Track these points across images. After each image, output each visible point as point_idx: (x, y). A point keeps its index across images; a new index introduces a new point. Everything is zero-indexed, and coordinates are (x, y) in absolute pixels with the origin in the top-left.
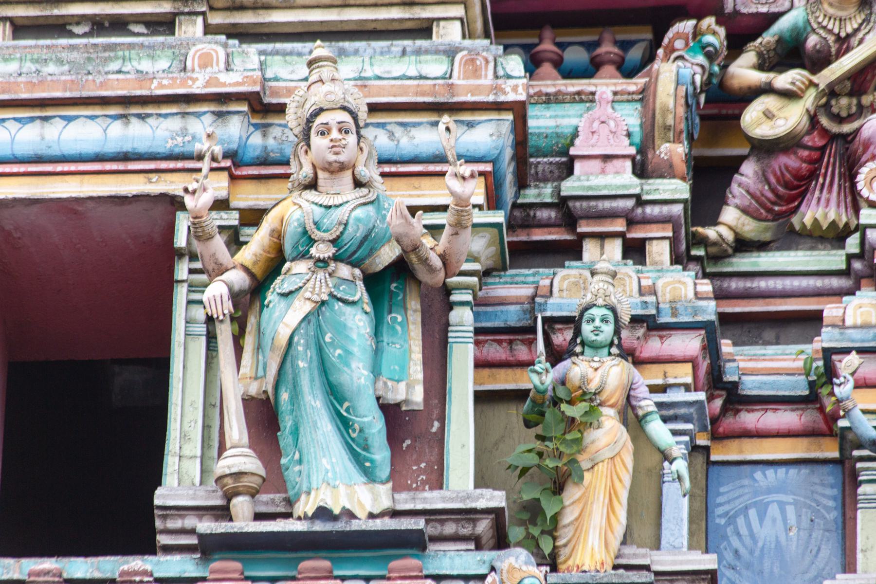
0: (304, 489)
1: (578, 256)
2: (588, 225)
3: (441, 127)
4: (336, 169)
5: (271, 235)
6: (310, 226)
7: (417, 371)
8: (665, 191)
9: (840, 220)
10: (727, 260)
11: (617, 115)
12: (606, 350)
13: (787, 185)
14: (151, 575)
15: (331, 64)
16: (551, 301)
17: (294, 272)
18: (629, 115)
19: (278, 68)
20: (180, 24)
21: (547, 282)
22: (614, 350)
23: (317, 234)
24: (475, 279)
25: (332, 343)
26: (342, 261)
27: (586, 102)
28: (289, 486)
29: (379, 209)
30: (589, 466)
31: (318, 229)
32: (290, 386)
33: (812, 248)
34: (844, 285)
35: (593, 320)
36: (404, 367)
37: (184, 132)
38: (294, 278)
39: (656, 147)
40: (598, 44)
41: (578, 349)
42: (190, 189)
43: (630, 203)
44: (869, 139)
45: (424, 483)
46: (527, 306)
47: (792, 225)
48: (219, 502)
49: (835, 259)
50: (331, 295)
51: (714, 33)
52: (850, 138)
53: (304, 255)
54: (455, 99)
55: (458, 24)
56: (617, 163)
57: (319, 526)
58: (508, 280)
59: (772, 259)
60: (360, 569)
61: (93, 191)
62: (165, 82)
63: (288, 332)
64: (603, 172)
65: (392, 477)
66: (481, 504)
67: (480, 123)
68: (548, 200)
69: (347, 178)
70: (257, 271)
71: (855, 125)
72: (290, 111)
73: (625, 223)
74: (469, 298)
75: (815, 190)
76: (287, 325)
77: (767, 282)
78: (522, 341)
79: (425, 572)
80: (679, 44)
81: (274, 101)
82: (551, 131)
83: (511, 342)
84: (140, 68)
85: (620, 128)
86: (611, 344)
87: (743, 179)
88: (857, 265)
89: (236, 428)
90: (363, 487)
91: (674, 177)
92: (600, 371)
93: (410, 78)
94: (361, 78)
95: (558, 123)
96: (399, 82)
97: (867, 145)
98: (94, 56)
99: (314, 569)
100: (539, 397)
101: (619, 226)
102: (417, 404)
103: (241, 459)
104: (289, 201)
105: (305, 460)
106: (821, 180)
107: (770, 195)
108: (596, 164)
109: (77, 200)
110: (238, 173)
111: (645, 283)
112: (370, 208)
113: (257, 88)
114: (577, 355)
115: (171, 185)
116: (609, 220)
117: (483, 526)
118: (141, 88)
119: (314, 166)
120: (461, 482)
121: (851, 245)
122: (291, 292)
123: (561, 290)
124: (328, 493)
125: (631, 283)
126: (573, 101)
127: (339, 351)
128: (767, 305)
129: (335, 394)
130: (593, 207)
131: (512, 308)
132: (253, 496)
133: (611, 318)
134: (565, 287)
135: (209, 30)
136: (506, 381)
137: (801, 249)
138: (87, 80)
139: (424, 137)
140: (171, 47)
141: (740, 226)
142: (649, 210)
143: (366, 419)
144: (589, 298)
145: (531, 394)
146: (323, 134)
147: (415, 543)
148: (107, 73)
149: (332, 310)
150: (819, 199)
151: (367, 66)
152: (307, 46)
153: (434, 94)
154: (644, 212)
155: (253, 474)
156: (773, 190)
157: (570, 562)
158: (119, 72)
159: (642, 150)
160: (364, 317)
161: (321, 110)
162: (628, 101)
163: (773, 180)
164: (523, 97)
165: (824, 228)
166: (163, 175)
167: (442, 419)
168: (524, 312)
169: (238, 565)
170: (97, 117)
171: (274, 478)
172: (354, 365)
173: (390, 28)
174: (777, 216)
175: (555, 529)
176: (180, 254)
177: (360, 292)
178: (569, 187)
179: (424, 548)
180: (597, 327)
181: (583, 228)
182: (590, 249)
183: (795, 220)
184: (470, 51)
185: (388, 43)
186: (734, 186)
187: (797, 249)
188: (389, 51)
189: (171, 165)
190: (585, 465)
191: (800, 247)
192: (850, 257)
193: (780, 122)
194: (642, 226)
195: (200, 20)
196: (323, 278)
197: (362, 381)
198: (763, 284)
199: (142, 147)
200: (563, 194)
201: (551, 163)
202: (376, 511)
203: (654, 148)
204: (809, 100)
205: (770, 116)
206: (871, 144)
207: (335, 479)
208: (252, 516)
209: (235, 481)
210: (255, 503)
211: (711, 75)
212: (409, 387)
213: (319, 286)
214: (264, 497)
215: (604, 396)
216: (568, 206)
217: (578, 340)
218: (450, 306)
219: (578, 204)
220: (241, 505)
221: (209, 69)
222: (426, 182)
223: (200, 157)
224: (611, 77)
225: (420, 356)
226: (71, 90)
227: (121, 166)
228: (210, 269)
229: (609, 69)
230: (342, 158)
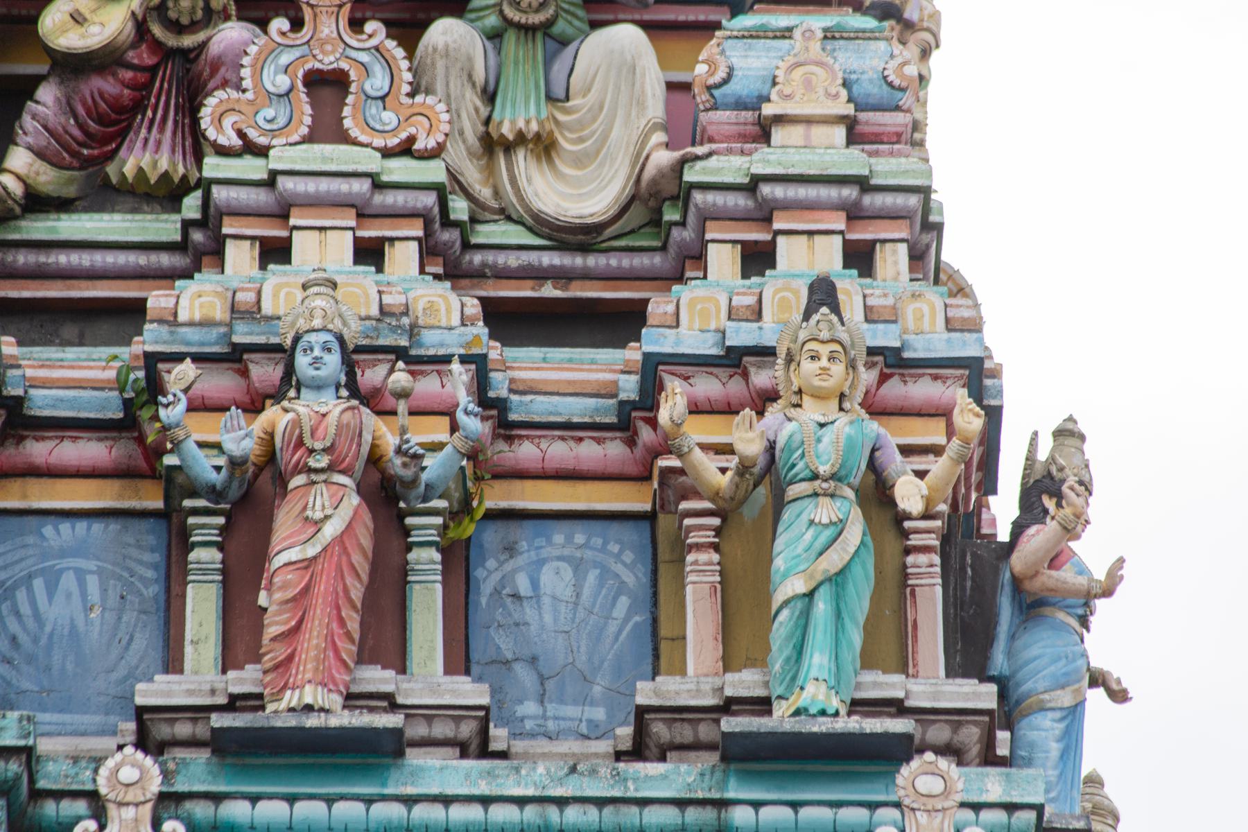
9: (176, 171)
10: (12, 223)
13: (101, 120)
33: (134, 211)
34: (178, 264)
44: (219, 57)
47: (107, 176)
49: (165, 227)
52: (192, 56)
59: (78, 224)
71: (201, 36)
75: (140, 128)
77: (68, 256)
87: (40, 108)
88: (197, 236)
97: (216, 66)
106: (149, 113)
107: (76, 132)
121: (189, 208)
128: (69, 289)
137: (119, 211)
141: (32, 175)
150: (146, 140)
156: (81, 126)
163: (81, 111)
165: (152, 182)
174: (85, 163)
183: (111, 169)
186: (27, 120)
187: (113, 211)
191: (117, 208)
192: (187, 225)
193: (94, 29)
198: (62, 259)
205: (80, 20)
206: (223, 64)
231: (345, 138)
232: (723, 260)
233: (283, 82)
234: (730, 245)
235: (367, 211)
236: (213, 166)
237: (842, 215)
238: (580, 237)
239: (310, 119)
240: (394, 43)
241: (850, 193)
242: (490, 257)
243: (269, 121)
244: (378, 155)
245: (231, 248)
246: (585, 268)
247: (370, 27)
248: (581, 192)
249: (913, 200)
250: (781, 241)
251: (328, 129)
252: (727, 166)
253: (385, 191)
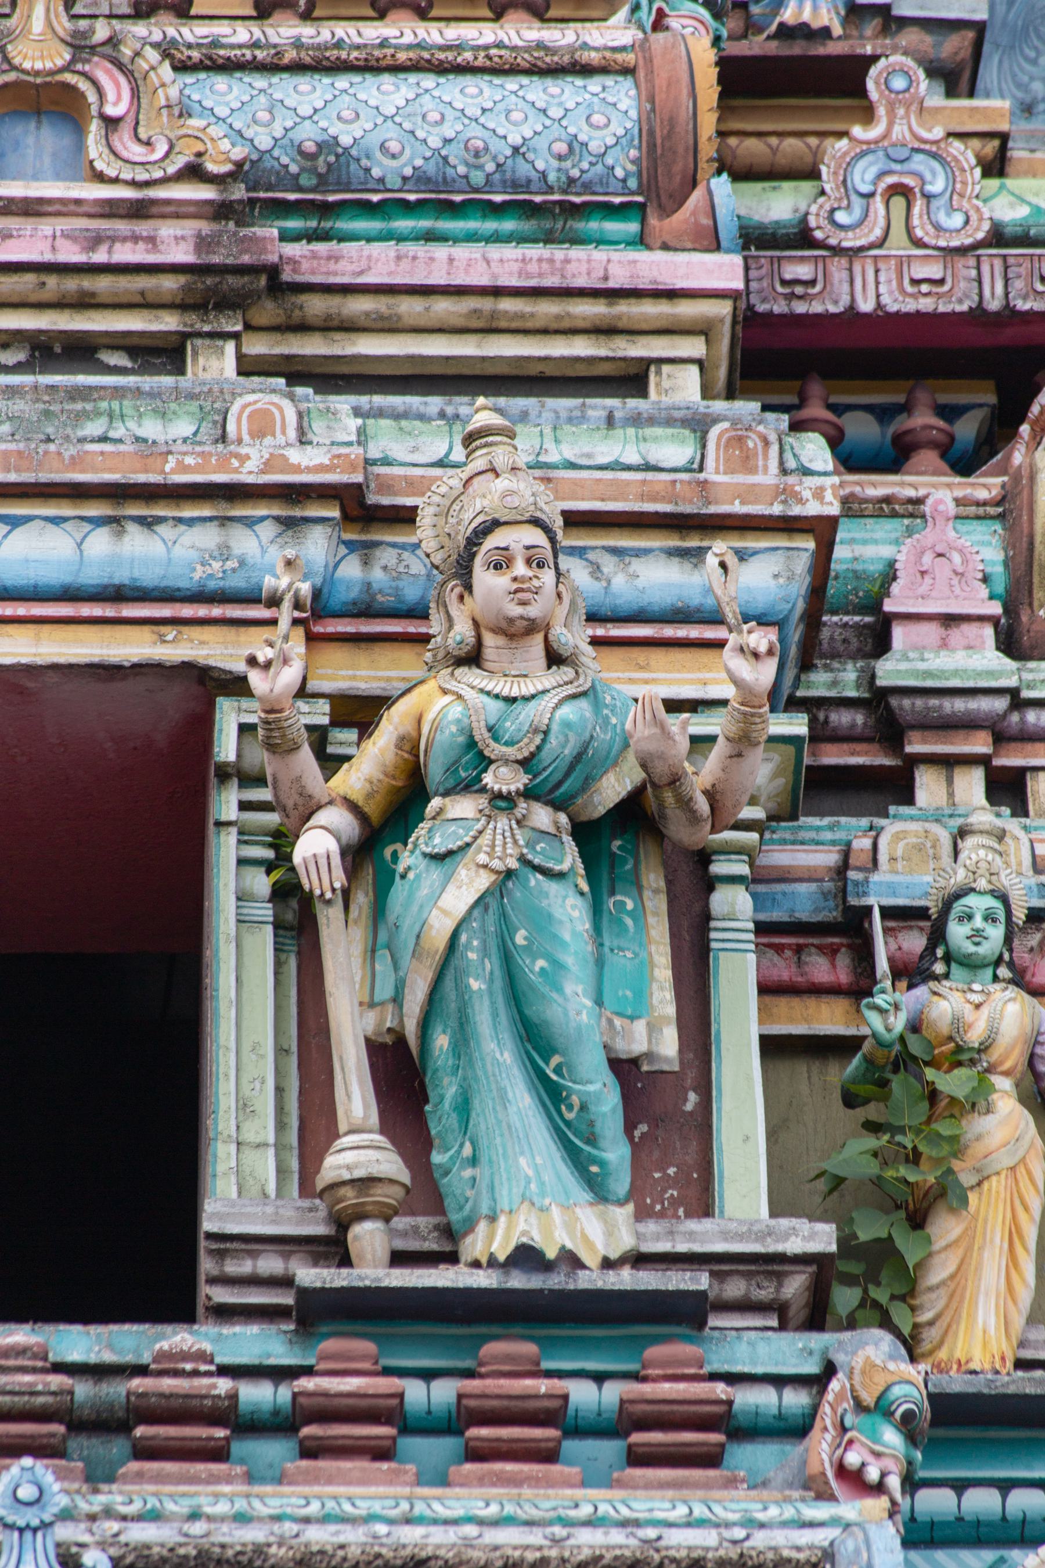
0: (485, 1210)
1: (908, 797)
2: (924, 742)
3: (712, 561)
4: (517, 631)
5: (399, 746)
6: (481, 734)
7: (664, 1000)
11: (965, 542)
12: (989, 972)
14: (212, 1362)
15: (505, 439)
16: (875, 878)
17: (451, 814)
18: (982, 543)
19: (389, 441)
20: (195, 353)
21: (866, 843)
22: (1004, 972)
23: (495, 749)
24: (755, 836)
25: (527, 948)
26: (537, 798)
27: (903, 516)
28: (449, 1203)
29: (597, 705)
30: (973, 1181)
31: (496, 739)
32: (453, 1023)
35: (970, 917)
36: (641, 995)
37: (224, 552)
38: (453, 828)
39: (1036, 603)
40: (906, 408)
41: (939, 968)
42: (261, 659)
43: (1000, 704)
45: (675, 1202)
46: (828, 885)
48: (320, 1229)
50: (523, 860)
53: (470, 786)
54: (712, 509)
55: (694, 370)
56: (969, 630)
57: (518, 1281)
58: (788, 836)
60: (587, 1359)
61: (59, 654)
62: (189, 460)
63: (450, 925)
64: (944, 644)
65: (635, 1194)
66: (794, 1246)
67: (755, 553)
68: (852, 693)
69: (536, 646)
70: (373, 810)
72: (425, 519)
73: (990, 740)
74: (744, 869)
76: (445, 912)
78: (820, 948)
79: (706, 1370)
81: (386, 501)
82: (844, 567)
83: (799, 950)
84: (141, 433)
85: (971, 566)
86: (998, 962)
89: (356, 1096)
90: (589, 1210)
92: (985, 1011)
93: (629, 468)
94: (538, 465)
95: (857, 554)
96: (608, 475)
98: (55, 408)
99: (509, 1358)
100: (880, 1055)
101: (980, 744)
102: (667, 1060)
103: (361, 1151)
104: (431, 685)
105: (484, 1159)
108: (931, 631)
109: (29, 670)
110: (318, 629)
112: (583, 704)
113: (358, 478)
114: (936, 978)
115: (216, 649)
116: (962, 733)
117: (795, 1286)
118: (146, 471)
119: (476, 624)
120: (745, 1206)
122: (450, 853)
123: (893, 859)
124: (533, 1221)
125: (1018, 849)
126: (879, 515)
127: (541, 963)
129: (535, 1040)
130: (934, 709)
131: (802, 888)
132: (387, 1220)
133: (1001, 915)
134: (899, 853)
135: (247, 367)
136: (791, 1020)
138: (46, 453)
139: (655, 576)
140: (192, 396)
142: (1032, 716)
143: (591, 1088)
144: (961, 876)
145: (867, 1046)
146: (498, 567)
147: (687, 1313)
148: (82, 440)
149: (525, 886)
151: (549, 444)
152: (461, 404)
153: (673, 499)
154: (1023, 720)
155: (392, 1181)
157: (943, 1354)
158: (104, 439)
159: (1011, 608)
160: (579, 901)
161: (494, 525)
162: (978, 518)
164: (834, 509)
166: (186, 630)
167: (705, 1088)
168: (825, 895)
169: (368, 1347)
170: (65, 519)
171: (426, 1191)
172: (569, 988)
173: (570, 372)
175: (912, 1293)
176: (224, 774)
177: (569, 857)
178: (890, 671)
179: (701, 1324)
180: (977, 931)
181: (915, 746)
182: (928, 787)
184: (735, 422)
185: (579, 401)
188: (583, 418)
189: (202, 611)
190: (967, 1179)
194: (1019, 745)
195: (230, 347)
196: (507, 828)
197: (584, 1016)
199: (149, 577)
200: (880, 682)
201: (845, 625)
202: (614, 1255)
203: (1031, 605)
207: (543, 1194)
208: (386, 1257)
209: (360, 1193)
210: (393, 1233)
212: (653, 1029)
213: (500, 843)
214: (400, 1222)
215: (994, 1055)
216: (888, 706)
217: (940, 952)
218: (710, 884)
219: (907, 702)
220: (368, 1237)
221: (268, 440)
222: (657, 656)
223: (274, 601)
224: (936, 473)
225: (669, 973)
226: (18, 470)
227: (109, 611)
228: (290, 804)
229: (928, 457)
230: (533, 611)
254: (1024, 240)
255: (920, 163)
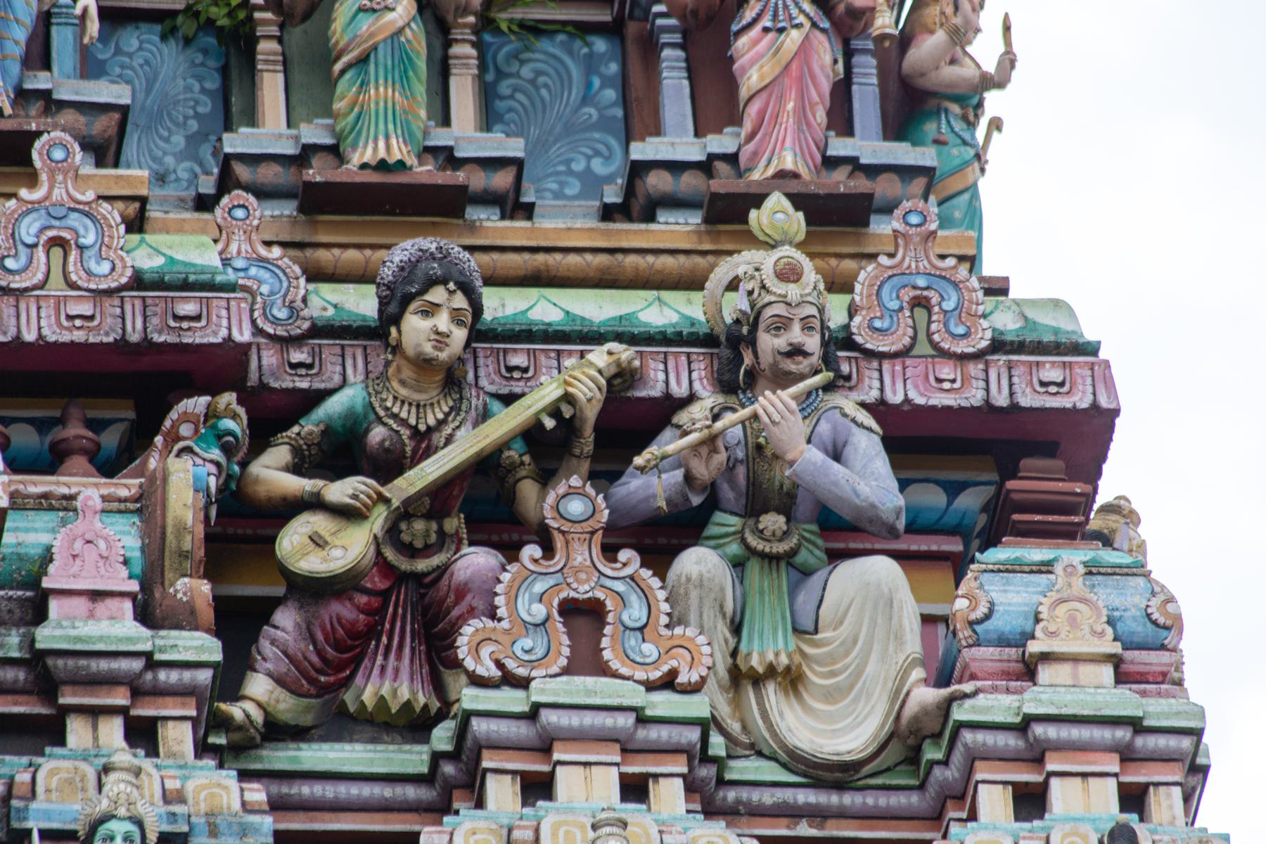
1: (61, 741)
2: (75, 695)
8: (186, 649)
9: (416, 700)
10: (253, 752)
11: (109, 531)
13: (338, 646)
16: (34, 806)
18: (123, 533)
21: (25, 777)
27: (59, 510)
33: (374, 740)
34: (424, 797)
39: (167, 583)
40: (61, 421)
44: (466, 584)
47: (343, 703)
49: (413, 758)
51: (235, 416)
52: (427, 580)
56: (112, 603)
59: (320, 754)
64: (91, 615)
68: (16, 654)
71: (436, 560)
73: (128, 694)
75: (376, 654)
77: (311, 787)
80: (185, 430)
82: (10, 550)
85: (114, 550)
87: (279, 633)
88: (448, 769)
91: (196, 628)
95: (20, 540)
97: (461, 592)
101: (120, 698)
106: (384, 639)
107: (315, 659)
108: (81, 604)
111: (170, 785)
116: (105, 688)
121: (440, 739)
123: (48, 791)
125: (151, 784)
126: (39, 508)
128: (311, 821)
130: (83, 668)
137: (357, 741)
141: (273, 702)
142: (162, 675)
144: (104, 805)
150: (383, 668)
154: (155, 678)
156: (319, 652)
159: (146, 586)
162: (120, 512)
163: (320, 636)
165: (393, 711)
174: (322, 690)
178: (46, 636)
181: (66, 699)
182: (77, 732)
183: (348, 697)
186: (265, 644)
187: (351, 741)
191: (356, 737)
192: (437, 757)
193: (337, 553)
194: (151, 699)
198: (306, 790)
200: (39, 646)
201: (11, 598)
203: (162, 584)
204: (378, 520)
205: (321, 542)
206: (469, 590)
211: (230, 477)
216: (45, 666)
219: (60, 662)
224: (84, 475)
229: (79, 461)
231: (603, 670)
232: (994, 802)
233: (539, 611)
234: (1000, 787)
235: (629, 747)
236: (471, 698)
237: (1116, 757)
238: (837, 775)
239: (568, 650)
240: (650, 573)
241: (1123, 734)
242: (744, 794)
243: (527, 652)
244: (642, 688)
245: (492, 783)
246: (841, 806)
247: (624, 555)
248: (842, 729)
249: (1186, 743)
250: (1054, 782)
251: (586, 661)
252: (996, 705)
253: (648, 726)
254: (159, 284)
255: (74, 220)
